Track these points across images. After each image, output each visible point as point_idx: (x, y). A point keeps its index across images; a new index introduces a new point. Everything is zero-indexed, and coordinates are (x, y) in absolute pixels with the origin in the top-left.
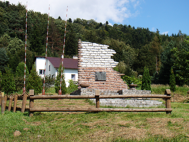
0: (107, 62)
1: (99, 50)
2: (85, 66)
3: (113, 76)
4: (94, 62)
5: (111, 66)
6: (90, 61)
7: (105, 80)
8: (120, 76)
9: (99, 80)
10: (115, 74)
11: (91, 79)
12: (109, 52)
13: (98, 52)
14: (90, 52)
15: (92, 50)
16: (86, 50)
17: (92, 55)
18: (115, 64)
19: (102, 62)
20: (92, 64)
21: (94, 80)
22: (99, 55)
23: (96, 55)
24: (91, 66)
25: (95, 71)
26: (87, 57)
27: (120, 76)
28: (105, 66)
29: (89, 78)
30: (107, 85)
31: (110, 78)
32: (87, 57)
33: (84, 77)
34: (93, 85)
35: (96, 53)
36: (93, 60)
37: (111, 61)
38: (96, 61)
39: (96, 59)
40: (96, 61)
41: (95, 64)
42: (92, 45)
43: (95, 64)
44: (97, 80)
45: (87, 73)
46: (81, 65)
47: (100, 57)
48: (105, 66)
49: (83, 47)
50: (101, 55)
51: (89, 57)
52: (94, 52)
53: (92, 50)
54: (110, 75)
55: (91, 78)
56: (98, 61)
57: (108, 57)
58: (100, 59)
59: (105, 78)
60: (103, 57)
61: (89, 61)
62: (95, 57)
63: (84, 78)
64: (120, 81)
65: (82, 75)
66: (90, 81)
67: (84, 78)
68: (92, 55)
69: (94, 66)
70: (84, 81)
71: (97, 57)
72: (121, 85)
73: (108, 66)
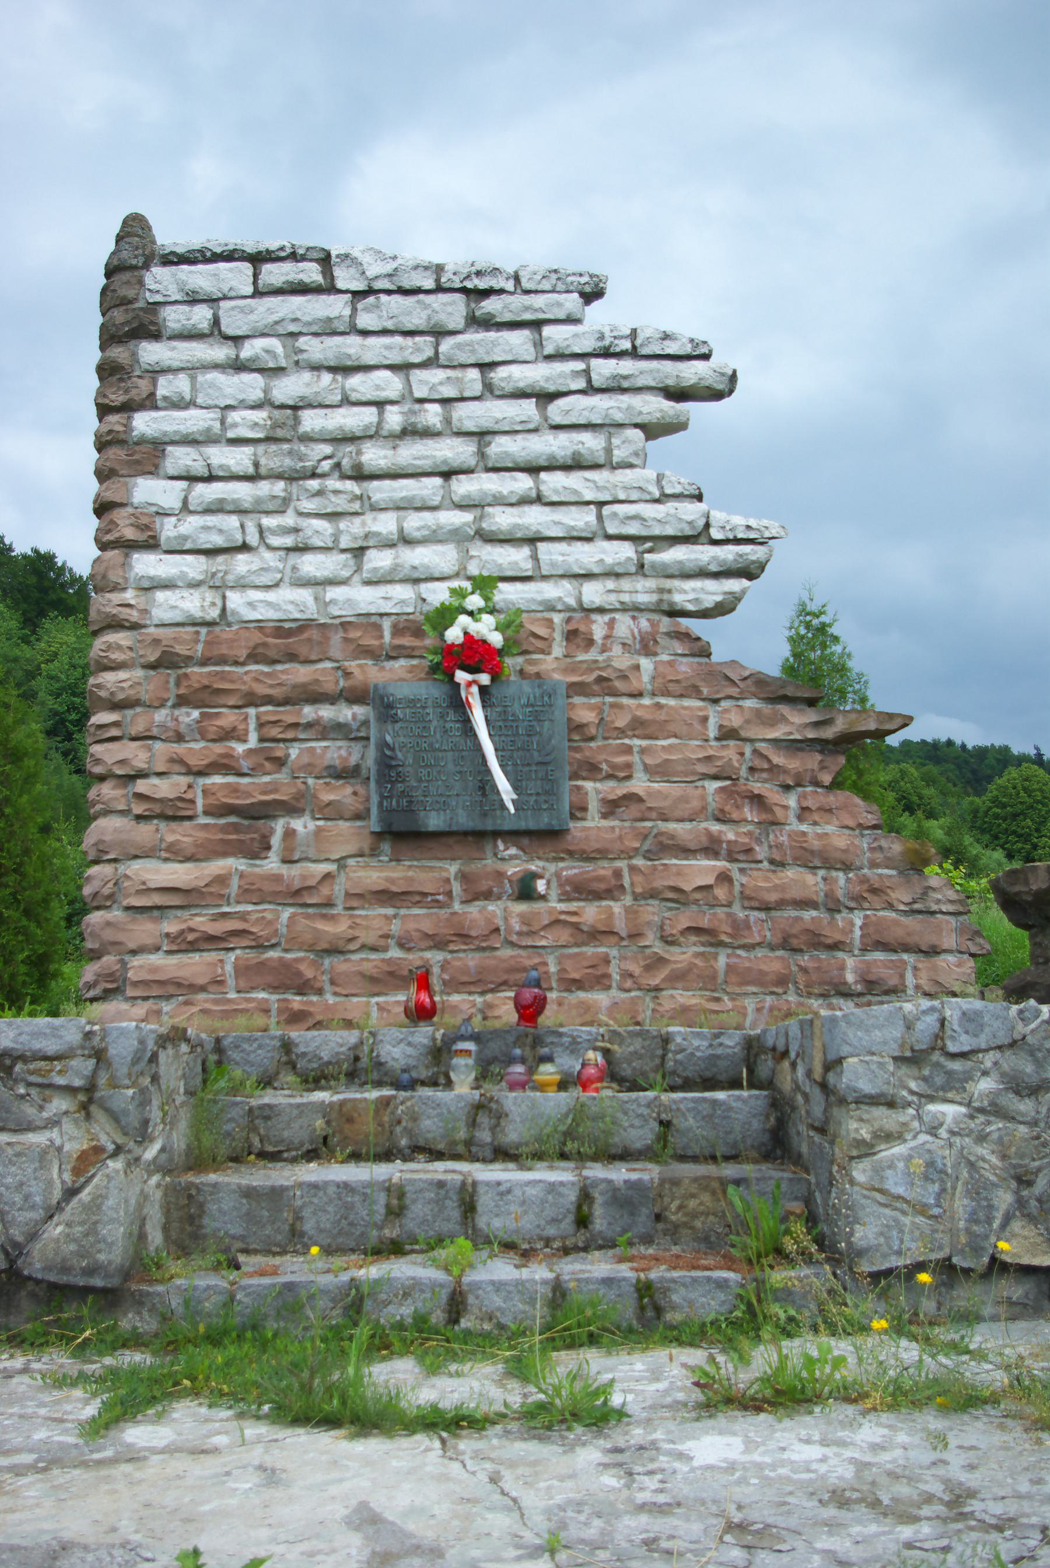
0: (583, 519)
1: (446, 345)
2: (193, 604)
3: (694, 750)
4: (352, 530)
5: (651, 583)
6: (289, 520)
7: (544, 821)
8: (824, 746)
9: (434, 821)
10: (735, 720)
11: (303, 825)
12: (603, 369)
13: (425, 381)
14: (290, 387)
15: (316, 349)
16: (221, 352)
17: (311, 421)
18: (728, 553)
19: (502, 519)
20: (311, 565)
21: (347, 836)
22: (432, 415)
23: (394, 418)
24: (291, 602)
25: (368, 672)
26: (239, 459)
27: (824, 746)
28: (550, 591)
29: (261, 813)
30: (590, 913)
31: (639, 784)
32: (239, 459)
33: (163, 788)
34: (340, 928)
35: (390, 384)
36: (340, 503)
37: (649, 511)
38: (386, 524)
39: (381, 490)
40: (386, 524)
41: (379, 560)
42: (312, 273)
43: (379, 560)
44: (402, 834)
45: (228, 718)
46: (129, 596)
47: (453, 451)
48: (550, 591)
49: (174, 317)
50: (469, 415)
51: (274, 458)
52: (359, 384)
53: (316, 349)
54: (638, 726)
55: (292, 809)
56: (414, 522)
57: (591, 443)
58: (464, 487)
59: (551, 791)
60: (501, 447)
61: (268, 522)
62: (374, 456)
63: (173, 812)
64: (832, 832)
65: (137, 755)
66: (271, 864)
67: (173, 812)
68: (311, 421)
69: (364, 598)
70: (176, 854)
71: (410, 453)
72: (858, 901)
73: (593, 593)
